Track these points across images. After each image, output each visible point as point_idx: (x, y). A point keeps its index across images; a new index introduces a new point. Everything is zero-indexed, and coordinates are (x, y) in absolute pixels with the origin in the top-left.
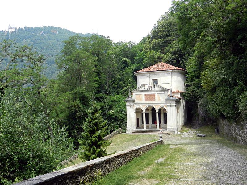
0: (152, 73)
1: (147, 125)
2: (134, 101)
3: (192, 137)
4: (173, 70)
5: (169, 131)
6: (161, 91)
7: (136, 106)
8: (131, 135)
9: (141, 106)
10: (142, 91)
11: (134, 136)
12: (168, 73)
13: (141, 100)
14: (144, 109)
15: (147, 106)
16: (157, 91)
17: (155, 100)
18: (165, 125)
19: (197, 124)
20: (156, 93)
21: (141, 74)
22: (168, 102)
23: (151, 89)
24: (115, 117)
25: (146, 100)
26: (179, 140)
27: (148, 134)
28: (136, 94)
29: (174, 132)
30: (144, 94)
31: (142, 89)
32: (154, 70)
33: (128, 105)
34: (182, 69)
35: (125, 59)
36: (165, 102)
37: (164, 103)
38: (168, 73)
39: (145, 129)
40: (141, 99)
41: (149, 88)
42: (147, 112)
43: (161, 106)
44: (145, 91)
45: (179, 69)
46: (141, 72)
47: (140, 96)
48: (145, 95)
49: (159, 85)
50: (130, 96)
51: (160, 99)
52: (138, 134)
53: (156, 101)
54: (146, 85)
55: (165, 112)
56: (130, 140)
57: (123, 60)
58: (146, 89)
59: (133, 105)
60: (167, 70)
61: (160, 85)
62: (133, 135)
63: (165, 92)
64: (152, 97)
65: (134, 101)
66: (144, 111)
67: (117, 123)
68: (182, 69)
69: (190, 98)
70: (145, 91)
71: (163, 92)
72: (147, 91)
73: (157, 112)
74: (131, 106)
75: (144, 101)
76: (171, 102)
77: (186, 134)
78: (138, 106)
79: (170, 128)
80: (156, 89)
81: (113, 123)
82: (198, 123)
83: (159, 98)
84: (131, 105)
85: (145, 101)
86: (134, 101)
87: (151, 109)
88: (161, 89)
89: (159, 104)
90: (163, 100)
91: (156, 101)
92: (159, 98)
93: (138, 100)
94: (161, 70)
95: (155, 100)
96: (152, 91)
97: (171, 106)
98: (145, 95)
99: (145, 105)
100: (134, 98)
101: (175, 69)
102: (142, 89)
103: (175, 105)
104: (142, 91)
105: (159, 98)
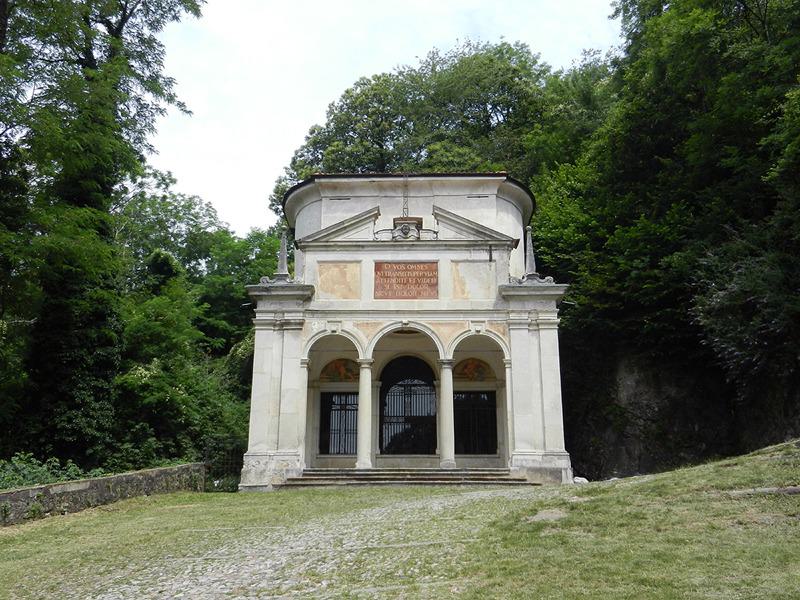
2: (308, 299)
5: (522, 467)
6: (471, 246)
7: (316, 327)
9: (348, 326)
10: (359, 246)
12: (480, 192)
13: (352, 292)
14: (365, 342)
15: (389, 324)
16: (449, 246)
19: (624, 457)
20: (444, 259)
22: (513, 306)
23: (413, 234)
24: (161, 403)
25: (382, 290)
28: (319, 262)
29: (556, 474)
30: (369, 259)
31: (364, 234)
33: (270, 317)
36: (496, 304)
37: (487, 312)
38: (480, 192)
39: (365, 458)
40: (350, 290)
44: (377, 245)
47: (344, 274)
48: (379, 266)
51: (467, 288)
52: (328, 488)
53: (444, 302)
57: (158, 255)
58: (386, 237)
59: (298, 317)
63: (495, 255)
64: (424, 279)
65: (306, 295)
66: (365, 354)
67: (167, 447)
70: (377, 245)
72: (394, 244)
73: (450, 363)
74: (288, 323)
75: (367, 300)
76: (530, 306)
78: (330, 328)
79: (529, 450)
80: (440, 237)
81: (137, 440)
82: (629, 453)
83: (461, 282)
84: (287, 316)
86: (306, 295)
89: (461, 318)
90: (486, 298)
91: (444, 302)
92: (464, 284)
93: (333, 291)
96: (418, 244)
97: (536, 326)
99: (370, 319)
100: (303, 279)
102: (364, 234)
104: (359, 246)
105: (461, 282)
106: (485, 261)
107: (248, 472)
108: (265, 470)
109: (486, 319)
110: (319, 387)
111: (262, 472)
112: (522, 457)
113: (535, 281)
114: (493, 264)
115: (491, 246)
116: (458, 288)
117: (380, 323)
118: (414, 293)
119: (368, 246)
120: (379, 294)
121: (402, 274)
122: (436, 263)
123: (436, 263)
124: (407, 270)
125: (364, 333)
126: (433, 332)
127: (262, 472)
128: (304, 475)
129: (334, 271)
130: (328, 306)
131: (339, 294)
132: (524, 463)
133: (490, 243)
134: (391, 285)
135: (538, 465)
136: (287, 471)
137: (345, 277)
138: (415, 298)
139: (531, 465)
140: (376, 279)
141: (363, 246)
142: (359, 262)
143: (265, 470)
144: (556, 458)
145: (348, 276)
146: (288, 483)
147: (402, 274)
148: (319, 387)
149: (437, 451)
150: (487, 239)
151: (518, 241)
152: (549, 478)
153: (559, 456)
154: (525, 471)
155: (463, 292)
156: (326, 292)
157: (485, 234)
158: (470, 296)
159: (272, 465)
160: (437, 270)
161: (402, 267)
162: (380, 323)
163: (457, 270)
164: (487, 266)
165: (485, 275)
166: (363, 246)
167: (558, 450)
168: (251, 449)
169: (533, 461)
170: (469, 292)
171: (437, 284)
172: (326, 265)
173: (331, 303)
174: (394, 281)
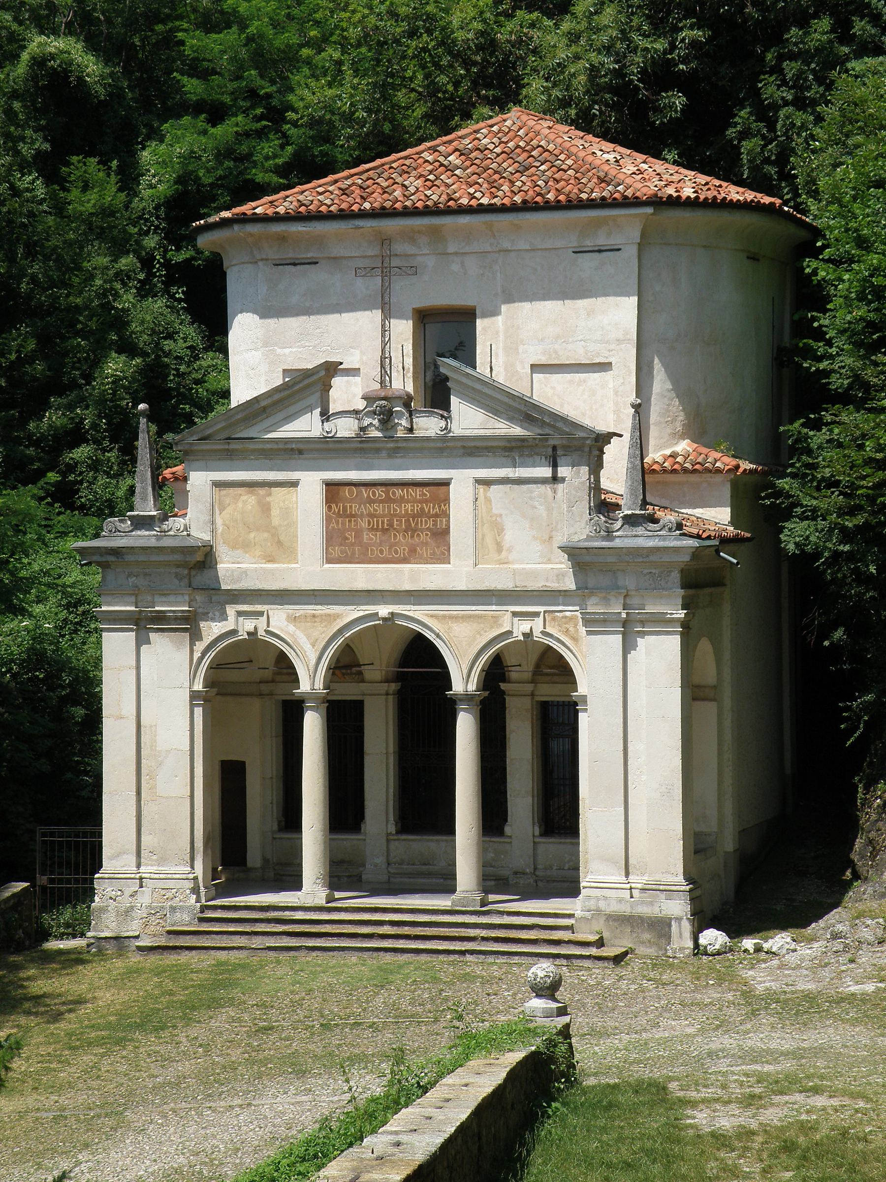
0: (411, 237)
1: (348, 839)
3: (870, 987)
4: (658, 203)
8: (153, 959)
11: (177, 972)
12: (602, 240)
17: (443, 557)
18: (552, 847)
21: (282, 239)
26: (723, 1026)
27: (354, 958)
32: (435, 196)
34: (767, 200)
35: (56, 44)
40: (280, 543)
41: (386, 418)
42: (348, 691)
43: (522, 627)
45: (735, 193)
46: (277, 218)
47: (265, 508)
49: (491, 385)
50: (147, 508)
51: (508, 538)
52: (233, 956)
54: (338, 382)
55: (548, 692)
56: (140, 1026)
58: (345, 428)
60: (591, 204)
61: (500, 377)
62: (172, 959)
63: (563, 471)
68: (767, 200)
69: (846, 535)
71: (547, 472)
73: (468, 698)
74: (160, 618)
77: (791, 959)
80: (457, 429)
85: (329, 561)
87: (396, 655)
88: (517, 431)
92: (499, 529)
93: (246, 546)
94: (527, 207)
95: (443, 557)
98: (330, 485)
101: (688, 192)
103: (681, 614)
106: (543, 481)
107: (103, 910)
108: (132, 908)
109: (541, 609)
110: (271, 694)
111: (128, 912)
112: (598, 893)
113: (640, 530)
114: (560, 487)
115: (554, 448)
116: (489, 541)
117: (338, 616)
118: (403, 550)
119: (312, 450)
120: (336, 552)
121: (379, 509)
122: (446, 483)
123: (446, 483)
124: (388, 500)
125: (308, 637)
126: (438, 636)
127: (128, 912)
128: (202, 920)
129: (248, 501)
130: (239, 580)
131: (258, 553)
132: (602, 905)
133: (551, 442)
134: (359, 533)
135: (625, 909)
136: (173, 909)
137: (269, 516)
138: (404, 561)
139: (614, 908)
140: (328, 520)
141: (300, 452)
142: (294, 484)
143: (132, 908)
144: (663, 896)
145: (275, 512)
146: (163, 942)
147: (380, 511)
148: (271, 694)
149: (507, 830)
150: (547, 431)
151: (605, 438)
152: (646, 936)
153: (669, 893)
154: (602, 920)
155: (499, 548)
156: (234, 548)
157: (543, 424)
158: (511, 558)
159: (145, 899)
160: (447, 500)
161: (380, 492)
162: (338, 616)
163: (488, 500)
164: (546, 489)
165: (542, 510)
166: (300, 452)
167: (671, 879)
168: (109, 865)
169: (620, 900)
170: (510, 550)
171: (446, 532)
172: (231, 491)
173: (245, 572)
174: (364, 524)
